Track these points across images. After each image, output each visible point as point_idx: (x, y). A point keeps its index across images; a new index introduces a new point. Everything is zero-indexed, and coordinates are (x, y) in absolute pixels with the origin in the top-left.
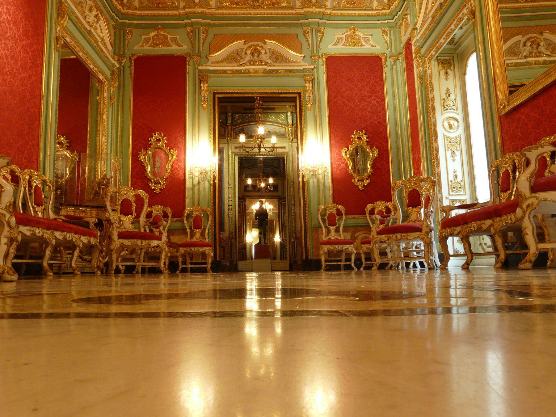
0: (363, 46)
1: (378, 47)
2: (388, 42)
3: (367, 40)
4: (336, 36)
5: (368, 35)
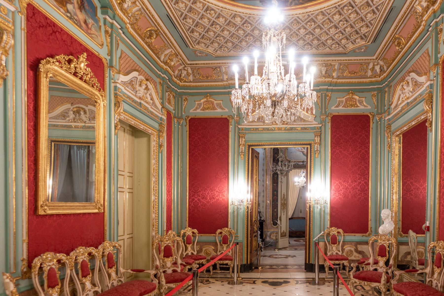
0: (358, 107)
1: (369, 107)
2: (376, 103)
3: (361, 102)
4: (338, 99)
5: (363, 98)
